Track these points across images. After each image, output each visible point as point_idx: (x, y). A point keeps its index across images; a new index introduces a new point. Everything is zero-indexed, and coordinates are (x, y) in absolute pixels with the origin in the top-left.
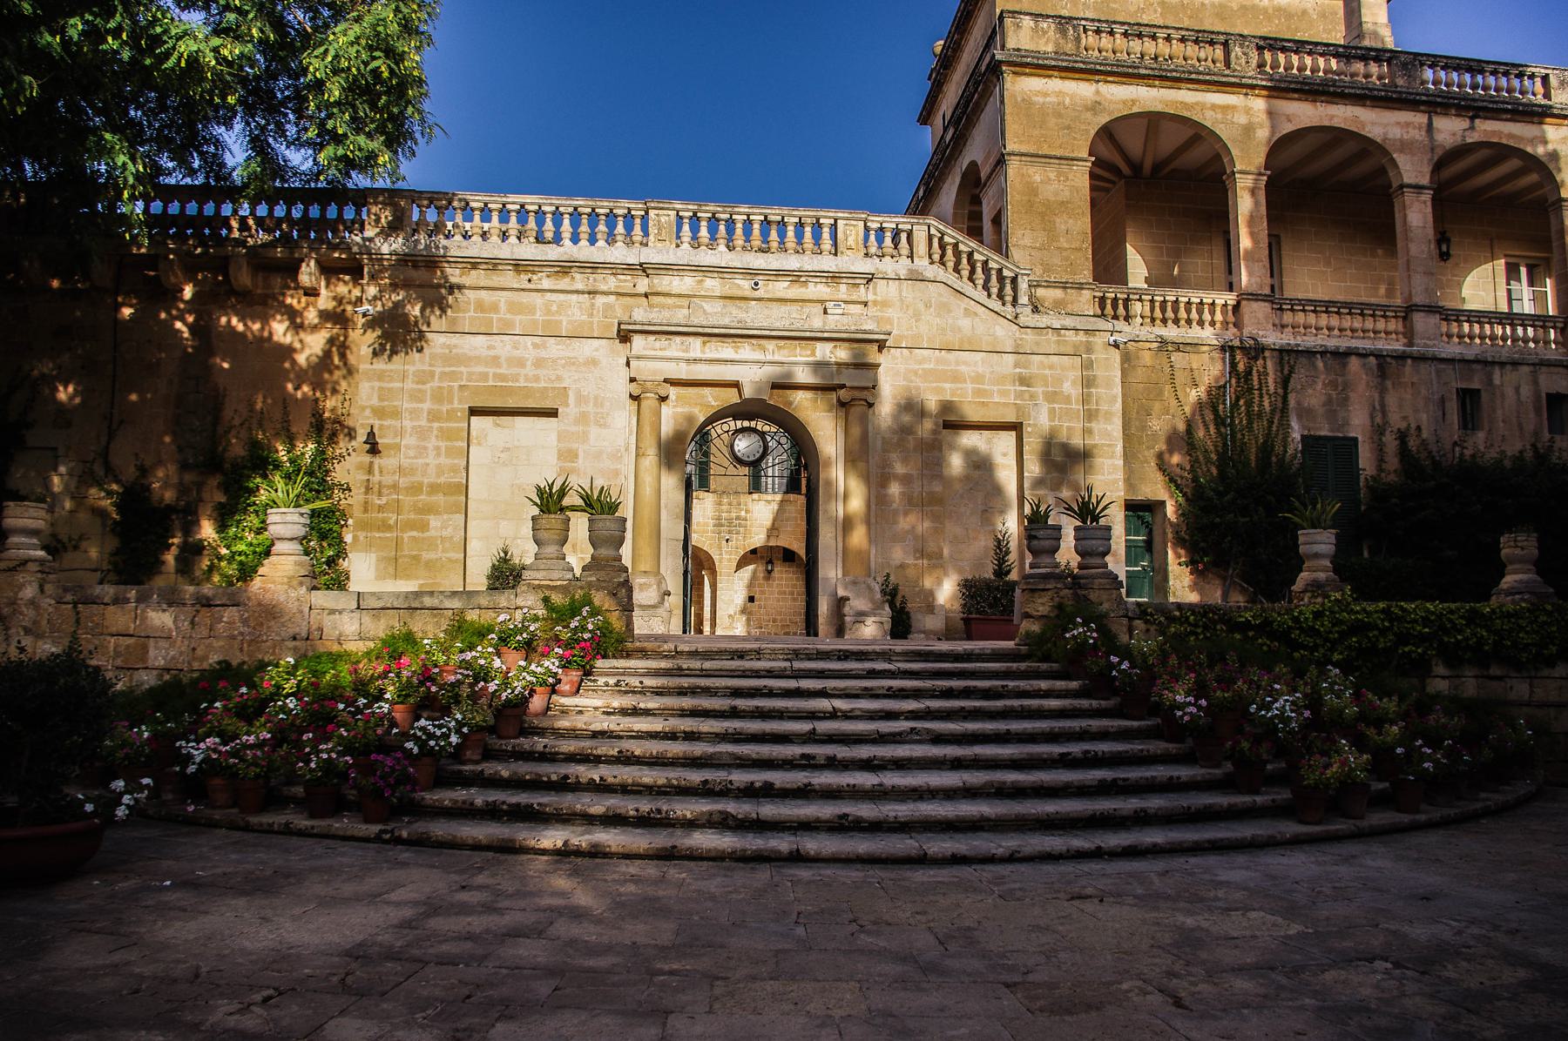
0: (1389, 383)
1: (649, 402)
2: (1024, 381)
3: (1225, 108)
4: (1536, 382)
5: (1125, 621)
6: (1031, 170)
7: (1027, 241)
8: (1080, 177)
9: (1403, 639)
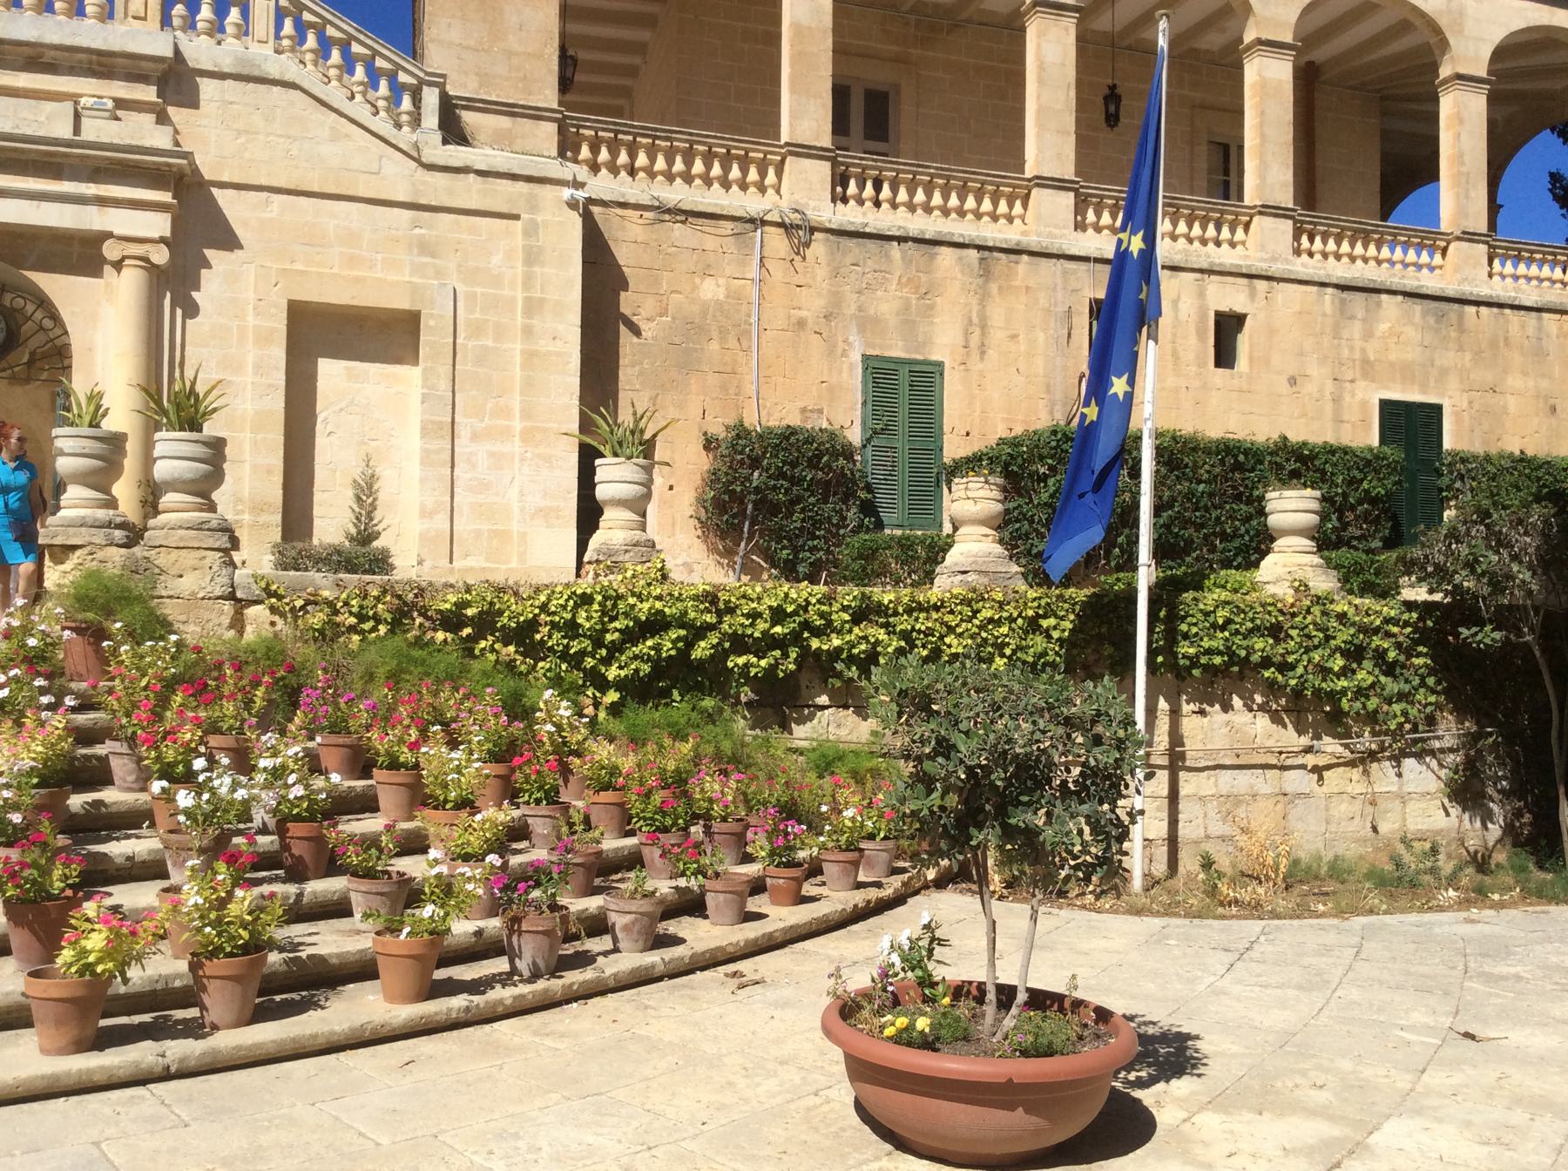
0: (994, 287)
2: (425, 248)
4: (1201, 294)
5: (228, 607)
7: (455, 35)
9: (740, 644)
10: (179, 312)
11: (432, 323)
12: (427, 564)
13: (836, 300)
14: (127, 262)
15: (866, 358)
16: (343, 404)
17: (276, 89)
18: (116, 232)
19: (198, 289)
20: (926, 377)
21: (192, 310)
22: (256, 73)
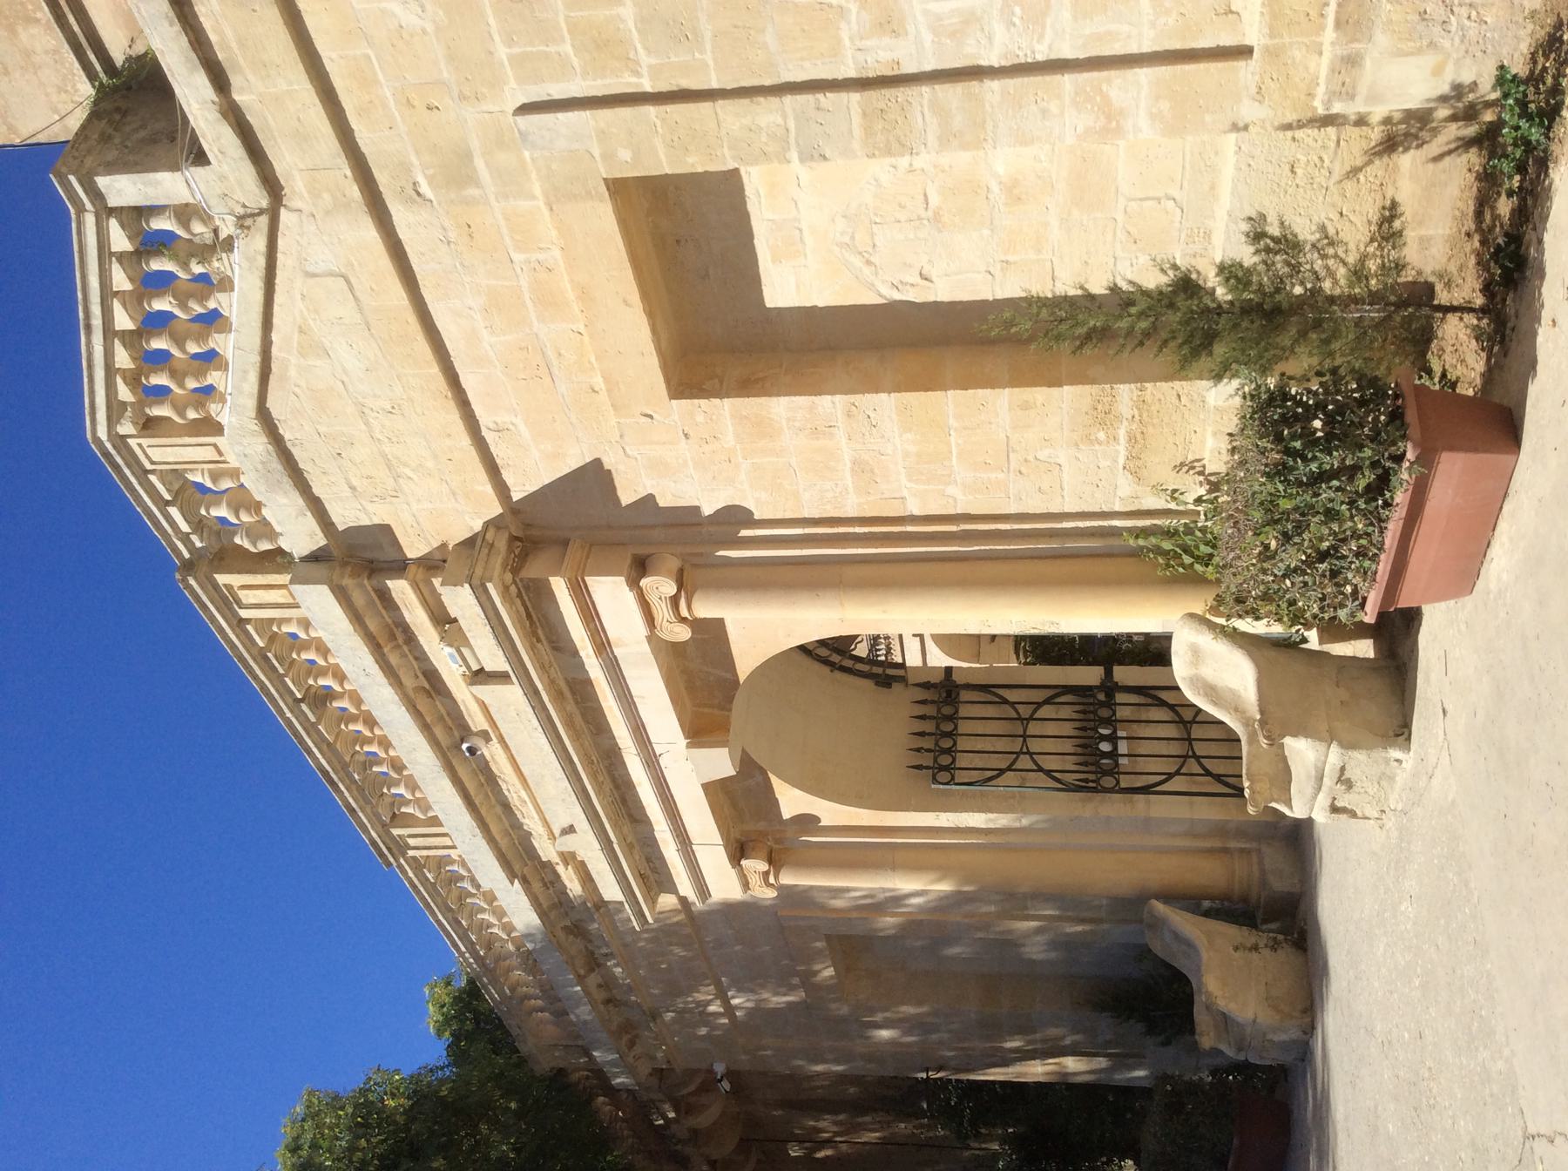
10: (744, 533)
11: (625, 155)
12: (1249, 111)
14: (684, 613)
16: (857, 262)
17: (286, 433)
18: (641, 629)
19: (697, 509)
21: (735, 517)
22: (276, 465)
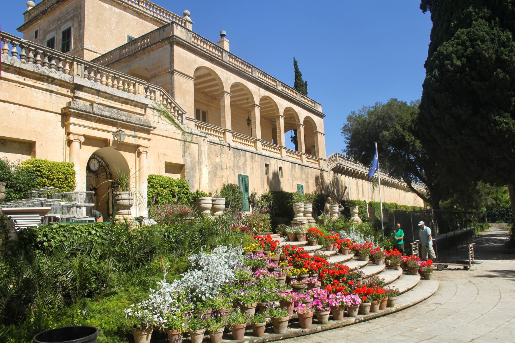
1: (76, 145)
3: (222, 71)
6: (180, 78)
8: (191, 83)
13: (234, 163)
15: (239, 175)
20: (247, 178)
